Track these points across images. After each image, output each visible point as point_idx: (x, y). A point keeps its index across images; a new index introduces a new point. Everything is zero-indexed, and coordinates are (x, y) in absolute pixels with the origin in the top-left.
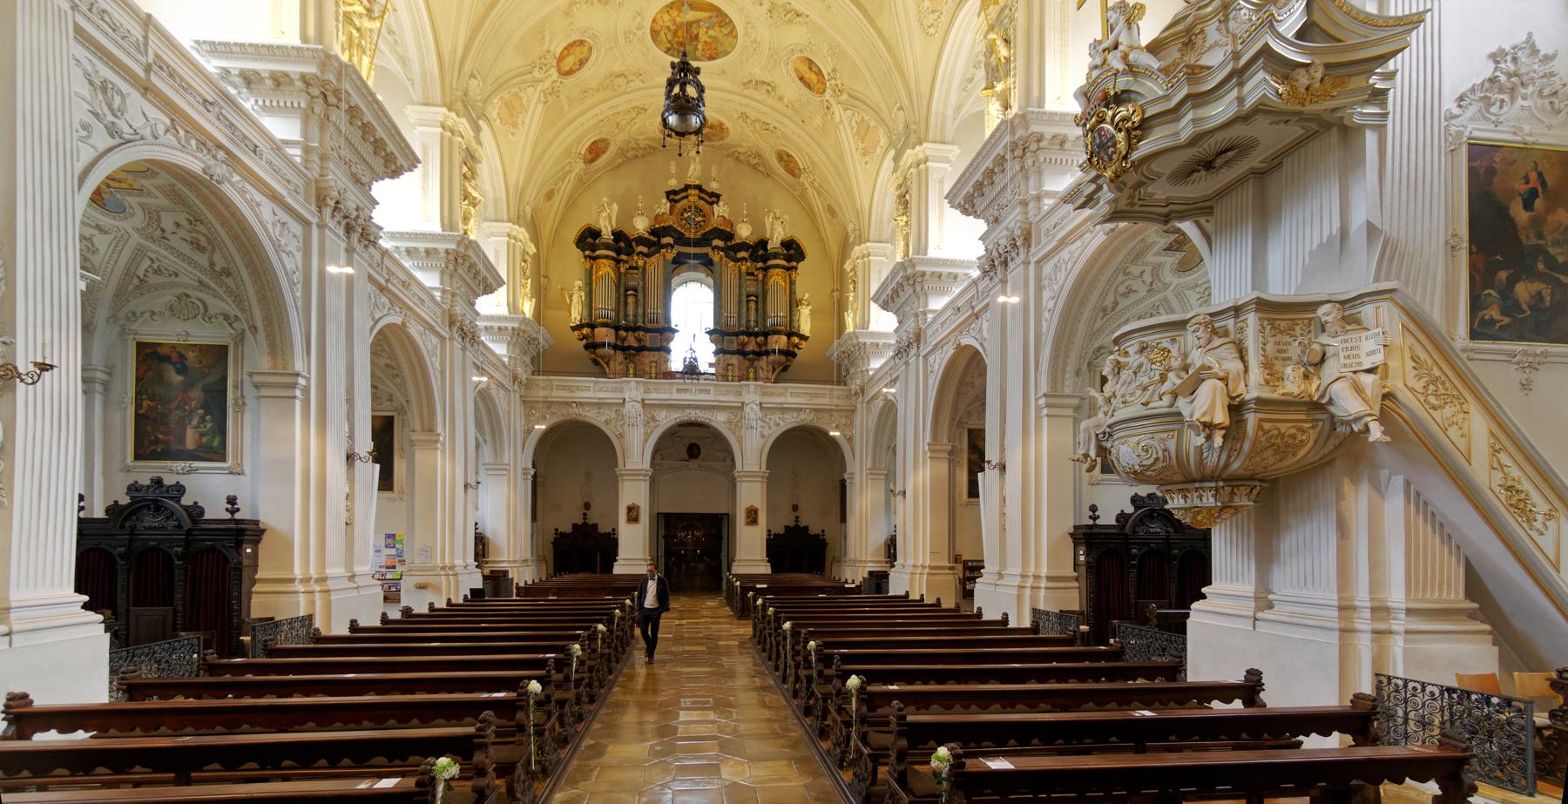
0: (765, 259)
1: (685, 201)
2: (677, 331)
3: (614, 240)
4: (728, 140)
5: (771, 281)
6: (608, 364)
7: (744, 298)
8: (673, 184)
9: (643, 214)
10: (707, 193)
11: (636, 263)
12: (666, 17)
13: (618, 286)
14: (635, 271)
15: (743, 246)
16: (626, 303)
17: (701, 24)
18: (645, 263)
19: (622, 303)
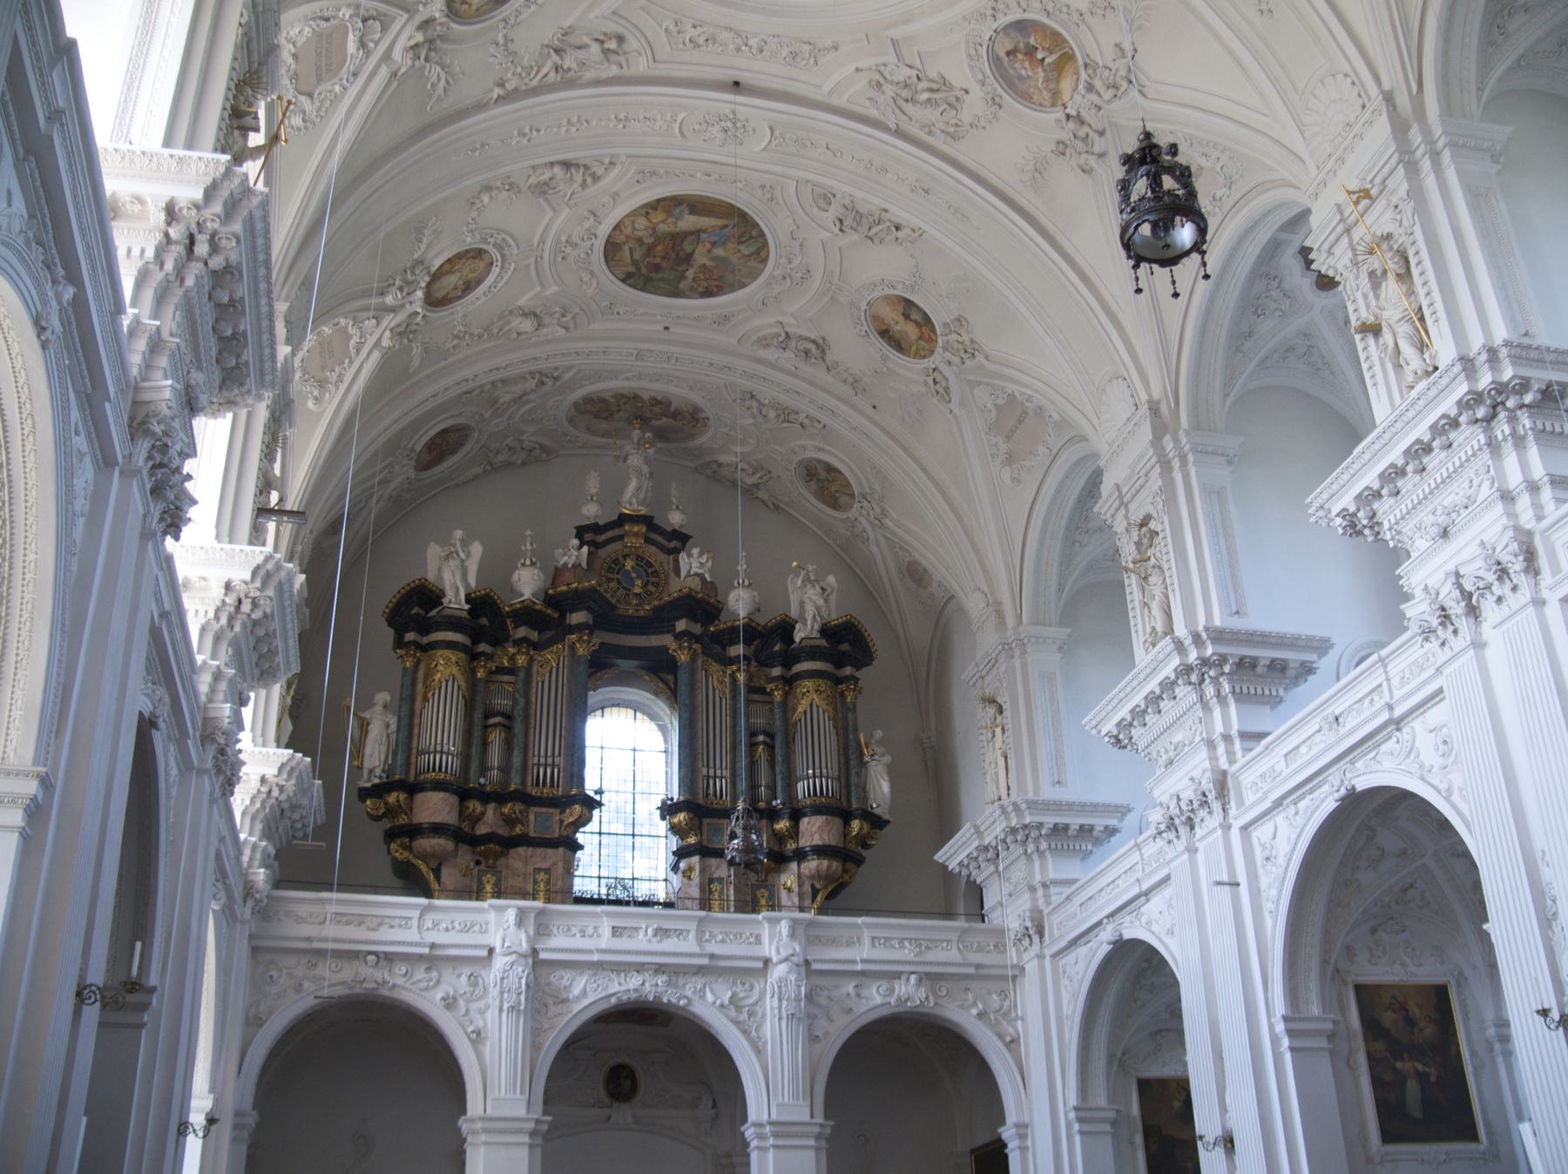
0: (788, 660)
1: (617, 546)
3: (470, 612)
4: (702, 440)
5: (803, 705)
8: (591, 511)
9: (533, 564)
10: (662, 532)
11: (512, 658)
12: (641, 223)
13: (469, 706)
14: (506, 678)
16: (485, 744)
17: (703, 236)
18: (531, 661)
19: (476, 741)
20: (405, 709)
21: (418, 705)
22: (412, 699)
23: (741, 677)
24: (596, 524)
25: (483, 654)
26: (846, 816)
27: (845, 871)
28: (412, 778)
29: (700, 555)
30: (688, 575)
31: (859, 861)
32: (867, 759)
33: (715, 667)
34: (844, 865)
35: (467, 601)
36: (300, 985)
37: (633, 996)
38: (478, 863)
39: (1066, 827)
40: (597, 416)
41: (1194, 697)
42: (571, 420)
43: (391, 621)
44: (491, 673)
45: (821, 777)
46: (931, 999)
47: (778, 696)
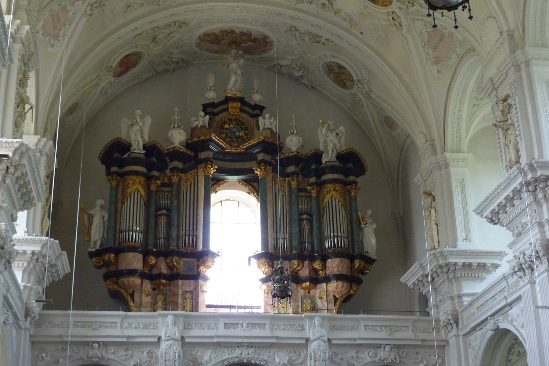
0: (319, 173)
1: (225, 114)
2: (218, 255)
3: (145, 154)
4: (270, 53)
5: (327, 198)
6: (132, 296)
7: (295, 216)
8: (211, 96)
9: (179, 127)
10: (250, 106)
11: (170, 178)
13: (147, 205)
15: (296, 159)
16: (156, 224)
18: (180, 180)
19: (152, 224)
20: (113, 209)
21: (119, 206)
22: (116, 203)
23: (294, 184)
24: (213, 103)
25: (154, 177)
26: (351, 258)
28: (117, 245)
29: (270, 118)
30: (264, 129)
31: (359, 282)
32: (363, 226)
35: (144, 149)
36: (58, 361)
37: (236, 360)
38: (154, 289)
39: (470, 265)
40: (212, 42)
41: (532, 198)
42: (198, 45)
43: (103, 163)
44: (158, 186)
45: (338, 237)
46: (398, 358)
47: (314, 193)
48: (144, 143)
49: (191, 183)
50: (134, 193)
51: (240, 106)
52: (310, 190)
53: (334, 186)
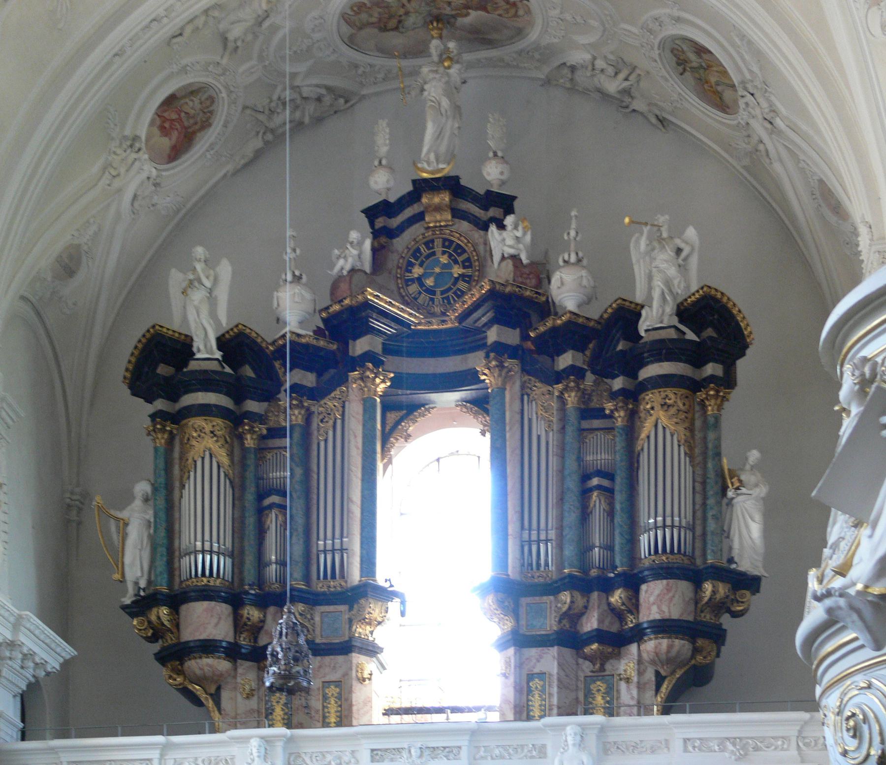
4: (534, 35)
5: (647, 427)
7: (572, 483)
10: (474, 197)
13: (238, 487)
16: (261, 532)
20: (161, 503)
23: (572, 399)
24: (385, 203)
27: (696, 651)
32: (730, 494)
33: (539, 388)
34: (693, 642)
35: (220, 348)
40: (384, 29)
42: (351, 42)
44: (263, 438)
45: (673, 526)
48: (220, 333)
49: (335, 423)
50: (203, 458)
51: (451, 201)
52: (612, 411)
53: (663, 395)
